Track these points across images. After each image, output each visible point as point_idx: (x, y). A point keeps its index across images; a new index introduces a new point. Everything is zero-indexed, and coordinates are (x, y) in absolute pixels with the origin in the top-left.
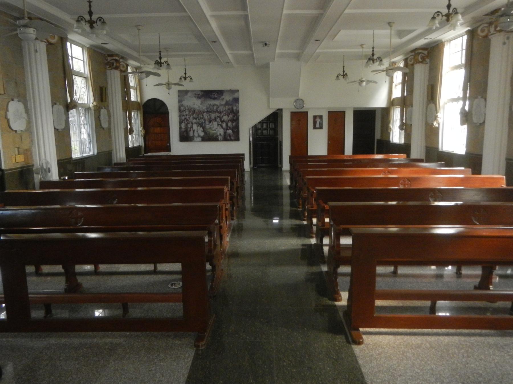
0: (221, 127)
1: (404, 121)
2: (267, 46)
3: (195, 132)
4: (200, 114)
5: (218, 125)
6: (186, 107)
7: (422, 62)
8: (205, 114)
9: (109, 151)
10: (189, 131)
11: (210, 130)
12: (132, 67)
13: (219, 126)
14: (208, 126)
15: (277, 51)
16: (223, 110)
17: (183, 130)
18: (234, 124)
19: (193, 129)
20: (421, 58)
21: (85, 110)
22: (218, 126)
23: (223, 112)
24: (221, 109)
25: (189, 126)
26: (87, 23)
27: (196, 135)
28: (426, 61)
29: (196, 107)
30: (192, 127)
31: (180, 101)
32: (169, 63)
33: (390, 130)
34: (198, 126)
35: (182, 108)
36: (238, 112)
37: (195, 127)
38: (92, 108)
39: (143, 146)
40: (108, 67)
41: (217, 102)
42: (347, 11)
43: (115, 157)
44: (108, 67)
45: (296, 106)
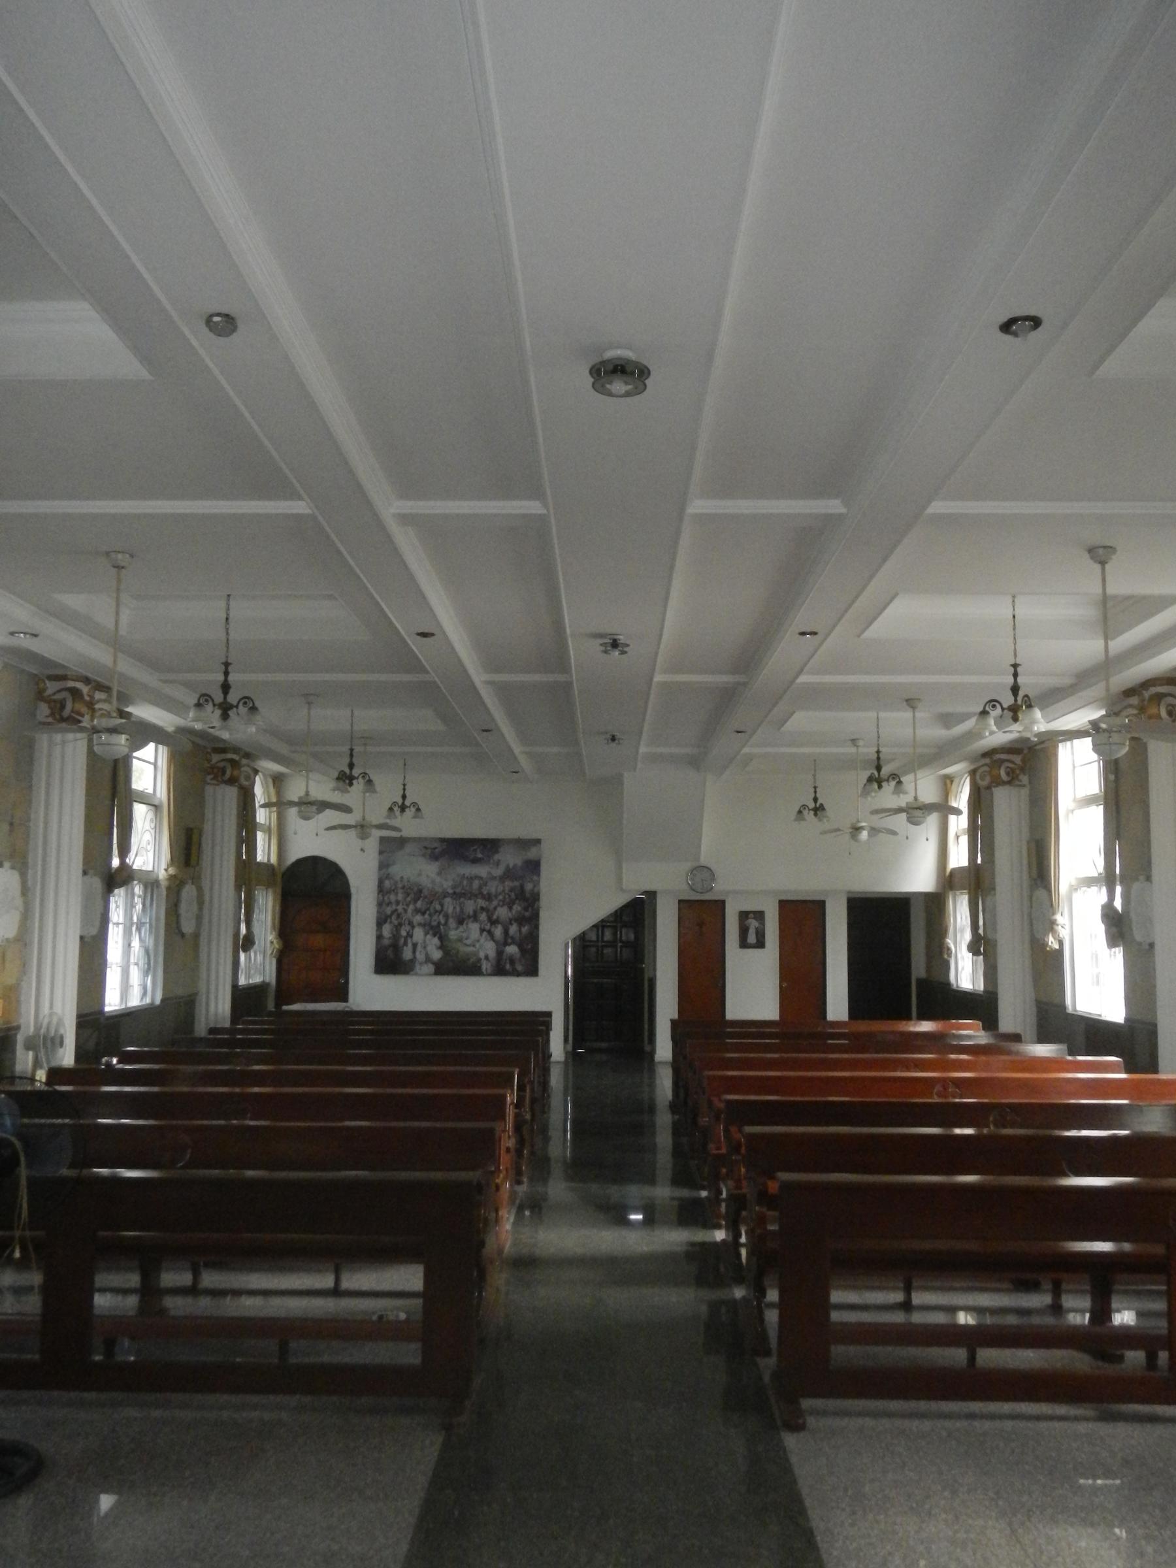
0: (489, 938)
1: (981, 931)
2: (617, 742)
3: (419, 948)
5: (482, 930)
6: (399, 883)
7: (1009, 783)
8: (448, 900)
9: (190, 996)
10: (403, 947)
11: (459, 944)
12: (264, 775)
13: (485, 933)
14: (453, 934)
15: (643, 749)
16: (496, 890)
17: (386, 942)
18: (525, 929)
19: (414, 941)
20: (1008, 774)
21: (146, 887)
22: (481, 935)
23: (496, 896)
24: (493, 887)
25: (404, 933)
26: (217, 707)
27: (420, 956)
28: (1020, 781)
29: (425, 882)
30: (409, 935)
31: (383, 866)
32: (371, 778)
33: (949, 955)
34: (426, 934)
35: (387, 884)
36: (536, 897)
37: (418, 934)
38: (164, 884)
39: (274, 982)
40: (212, 779)
41: (482, 871)
42: (803, 679)
43: (204, 1011)
44: (212, 779)
45: (693, 884)
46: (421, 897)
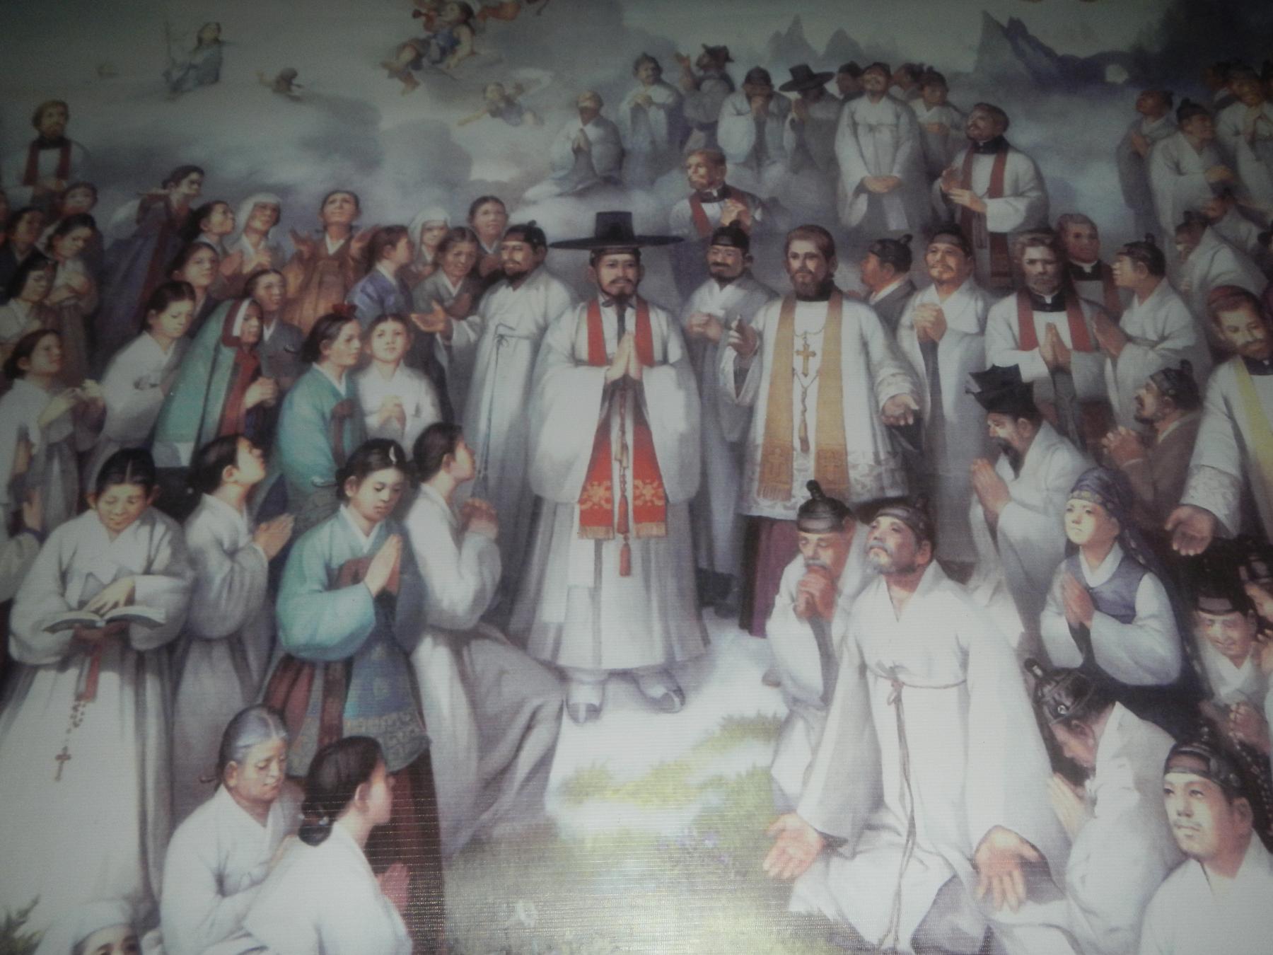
4: (341, 314)
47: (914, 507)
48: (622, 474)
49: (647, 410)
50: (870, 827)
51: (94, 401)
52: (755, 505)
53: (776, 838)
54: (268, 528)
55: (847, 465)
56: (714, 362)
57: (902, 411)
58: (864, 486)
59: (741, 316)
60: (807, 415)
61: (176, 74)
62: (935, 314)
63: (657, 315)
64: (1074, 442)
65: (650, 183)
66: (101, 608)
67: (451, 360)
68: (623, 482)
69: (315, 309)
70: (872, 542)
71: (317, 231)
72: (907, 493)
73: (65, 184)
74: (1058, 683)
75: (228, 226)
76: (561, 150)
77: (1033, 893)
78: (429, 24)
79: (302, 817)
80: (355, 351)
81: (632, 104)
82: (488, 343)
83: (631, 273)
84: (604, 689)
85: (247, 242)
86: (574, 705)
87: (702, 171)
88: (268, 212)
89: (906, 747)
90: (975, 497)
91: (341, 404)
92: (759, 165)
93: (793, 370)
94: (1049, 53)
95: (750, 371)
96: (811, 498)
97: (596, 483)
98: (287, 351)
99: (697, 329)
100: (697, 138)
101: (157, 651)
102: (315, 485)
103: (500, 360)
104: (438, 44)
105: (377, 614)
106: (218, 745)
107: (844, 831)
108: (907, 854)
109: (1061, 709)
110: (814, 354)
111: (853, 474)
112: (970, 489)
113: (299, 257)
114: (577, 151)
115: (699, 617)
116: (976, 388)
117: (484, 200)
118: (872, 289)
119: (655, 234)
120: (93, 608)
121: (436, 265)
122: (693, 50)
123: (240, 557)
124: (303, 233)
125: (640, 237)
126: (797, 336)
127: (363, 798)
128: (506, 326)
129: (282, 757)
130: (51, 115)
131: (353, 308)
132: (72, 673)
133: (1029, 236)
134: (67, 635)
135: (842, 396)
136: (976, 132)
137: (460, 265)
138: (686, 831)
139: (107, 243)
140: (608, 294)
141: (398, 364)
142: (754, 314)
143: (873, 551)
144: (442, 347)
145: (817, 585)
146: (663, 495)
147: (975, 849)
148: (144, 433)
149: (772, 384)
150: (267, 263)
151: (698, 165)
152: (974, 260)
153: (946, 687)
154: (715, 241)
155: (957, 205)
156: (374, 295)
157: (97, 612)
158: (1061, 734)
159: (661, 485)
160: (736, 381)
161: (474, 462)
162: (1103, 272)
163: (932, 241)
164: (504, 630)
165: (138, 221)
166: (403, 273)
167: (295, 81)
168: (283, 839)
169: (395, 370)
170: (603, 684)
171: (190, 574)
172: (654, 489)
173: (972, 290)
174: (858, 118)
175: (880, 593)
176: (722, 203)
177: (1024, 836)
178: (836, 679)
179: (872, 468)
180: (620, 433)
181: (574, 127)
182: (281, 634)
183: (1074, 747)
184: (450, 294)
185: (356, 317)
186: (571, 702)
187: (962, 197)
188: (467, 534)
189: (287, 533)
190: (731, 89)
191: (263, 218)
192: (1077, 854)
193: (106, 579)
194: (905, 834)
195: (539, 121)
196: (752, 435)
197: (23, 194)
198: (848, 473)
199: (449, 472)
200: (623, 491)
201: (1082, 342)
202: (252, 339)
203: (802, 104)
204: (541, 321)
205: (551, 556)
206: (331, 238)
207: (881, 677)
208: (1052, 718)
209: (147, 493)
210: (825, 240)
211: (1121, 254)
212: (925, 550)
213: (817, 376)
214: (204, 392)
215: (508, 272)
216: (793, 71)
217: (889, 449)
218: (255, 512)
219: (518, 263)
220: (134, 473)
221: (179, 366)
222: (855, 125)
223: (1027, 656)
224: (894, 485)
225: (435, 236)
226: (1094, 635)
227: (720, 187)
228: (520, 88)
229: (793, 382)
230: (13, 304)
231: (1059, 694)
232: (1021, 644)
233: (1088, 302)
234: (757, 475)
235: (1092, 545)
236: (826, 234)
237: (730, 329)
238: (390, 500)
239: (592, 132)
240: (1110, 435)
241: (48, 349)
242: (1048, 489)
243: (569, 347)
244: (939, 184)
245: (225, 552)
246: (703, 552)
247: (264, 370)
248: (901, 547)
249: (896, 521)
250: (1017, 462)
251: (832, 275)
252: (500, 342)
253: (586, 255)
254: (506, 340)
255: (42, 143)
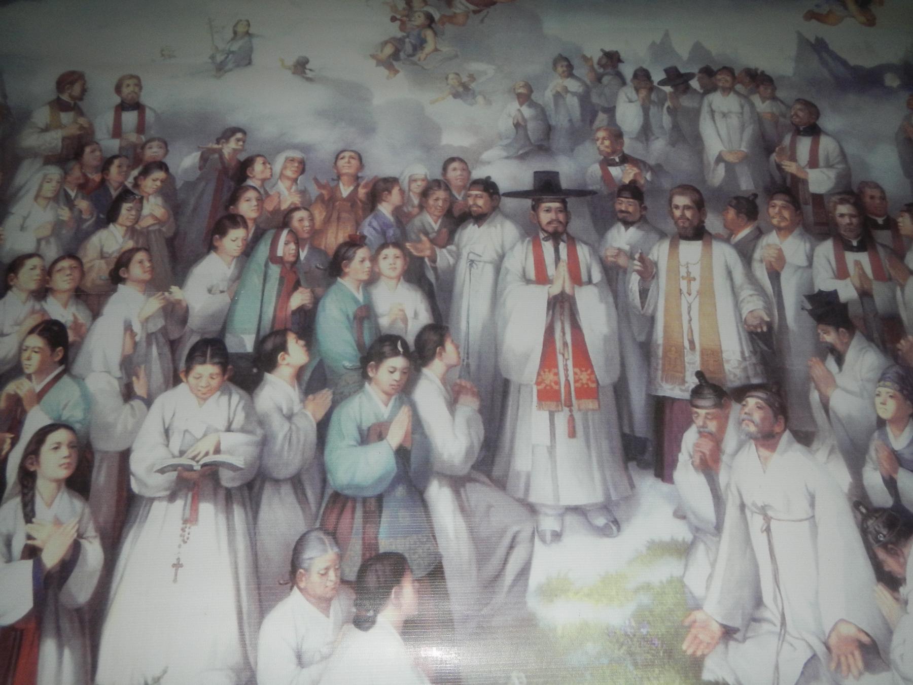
4: (355, 242)
6: (42, 116)
46: (237, 220)
47: (771, 391)
48: (565, 363)
49: (580, 318)
50: (756, 620)
51: (179, 302)
52: (660, 388)
53: (690, 627)
54: (314, 399)
55: (722, 360)
56: (624, 283)
57: (758, 322)
58: (735, 375)
59: (641, 250)
60: (693, 322)
61: (220, 58)
62: (777, 252)
63: (582, 248)
64: (878, 346)
65: (571, 151)
66: (199, 454)
67: (437, 278)
68: (566, 370)
69: (336, 238)
70: (743, 416)
71: (333, 180)
72: (765, 381)
73: (143, 138)
74: (877, 518)
75: (267, 174)
76: (505, 124)
77: (869, 666)
78: (402, 28)
79: (354, 610)
80: (367, 270)
81: (554, 92)
82: (463, 265)
83: (561, 217)
84: (562, 520)
85: (282, 187)
86: (542, 531)
87: (607, 143)
88: (296, 165)
89: (776, 564)
90: (813, 385)
91: (361, 308)
92: (647, 140)
93: (681, 290)
94: (844, 63)
95: (650, 290)
96: (699, 383)
97: (547, 370)
98: (318, 268)
99: (612, 259)
100: (602, 118)
101: (240, 488)
102: (345, 368)
103: (472, 278)
104: (410, 42)
105: (397, 463)
106: (290, 558)
107: (736, 623)
108: (781, 639)
109: (880, 537)
110: (694, 279)
111: (727, 367)
112: (809, 378)
113: (321, 198)
114: (517, 125)
115: (626, 468)
116: (809, 307)
117: (452, 160)
118: (732, 233)
119: (577, 189)
120: (191, 456)
121: (422, 207)
122: (594, 53)
123: (296, 419)
124: (323, 181)
125: (566, 190)
126: (682, 266)
127: (397, 598)
128: (474, 253)
129: (337, 567)
130: (128, 85)
131: (363, 237)
132: (179, 503)
133: (839, 197)
134: (173, 475)
135: (716, 310)
136: (797, 120)
137: (439, 208)
138: (627, 622)
139: (179, 184)
140: (546, 231)
141: (399, 280)
142: (650, 249)
143: (744, 422)
144: (430, 268)
145: (707, 446)
146: (594, 379)
147: (827, 635)
148: (218, 327)
149: (666, 300)
150: (297, 202)
151: (604, 139)
152: (801, 213)
153: (801, 520)
154: (619, 195)
155: (787, 173)
156: (378, 228)
157: (193, 458)
158: (882, 555)
159: (593, 372)
160: (641, 298)
161: (459, 353)
162: (891, 224)
163: (772, 199)
164: (489, 476)
165: (201, 168)
166: (398, 212)
167: (308, 66)
168: (343, 625)
169: (397, 284)
170: (562, 516)
171: (259, 432)
172: (588, 375)
173: (801, 234)
174: (714, 107)
175: (751, 453)
176: (622, 167)
177: (860, 626)
178: (724, 514)
179: (740, 363)
180: (562, 334)
181: (513, 107)
182: (329, 476)
183: (891, 564)
184: (433, 229)
185: (366, 245)
186: (540, 529)
187: (790, 167)
188: (458, 406)
189: (328, 403)
190: (624, 83)
191: (293, 169)
192: (896, 639)
193: (199, 435)
194: (778, 624)
195: (489, 102)
196: (654, 337)
197: (113, 145)
198: (723, 366)
199: (441, 360)
200: (567, 376)
201: (880, 274)
202: (292, 259)
203: (675, 95)
204: (500, 250)
205: (519, 423)
206: (344, 185)
207: (756, 513)
208: (875, 543)
209: (224, 371)
210: (697, 196)
211: (902, 211)
212: (780, 422)
213: (697, 295)
214: (260, 298)
215: (473, 213)
216: (667, 71)
217: (751, 349)
218: (304, 387)
219: (480, 207)
220: (212, 356)
221: (239, 277)
222: (712, 112)
223: (855, 499)
224: (756, 375)
225: (418, 186)
226: (900, 484)
227: (620, 155)
228: (472, 78)
229: (681, 299)
230: (111, 226)
231: (879, 527)
232: (850, 490)
233: (883, 246)
234: (660, 367)
235: (894, 421)
236: (698, 192)
237: (634, 259)
238: (401, 379)
239: (527, 112)
240: (902, 342)
241: (141, 262)
242: (862, 380)
243: (521, 270)
244: (774, 157)
245: (284, 415)
246: (626, 422)
247: (302, 282)
248: (763, 420)
249: (760, 401)
250: (840, 360)
251: (703, 222)
252: (471, 265)
253: (528, 202)
254: (476, 264)
255: (123, 107)
